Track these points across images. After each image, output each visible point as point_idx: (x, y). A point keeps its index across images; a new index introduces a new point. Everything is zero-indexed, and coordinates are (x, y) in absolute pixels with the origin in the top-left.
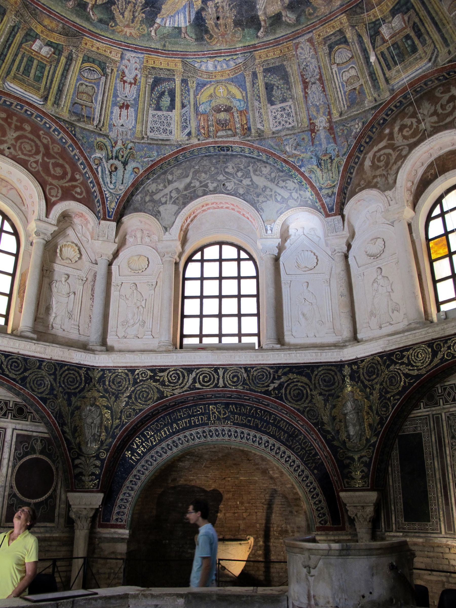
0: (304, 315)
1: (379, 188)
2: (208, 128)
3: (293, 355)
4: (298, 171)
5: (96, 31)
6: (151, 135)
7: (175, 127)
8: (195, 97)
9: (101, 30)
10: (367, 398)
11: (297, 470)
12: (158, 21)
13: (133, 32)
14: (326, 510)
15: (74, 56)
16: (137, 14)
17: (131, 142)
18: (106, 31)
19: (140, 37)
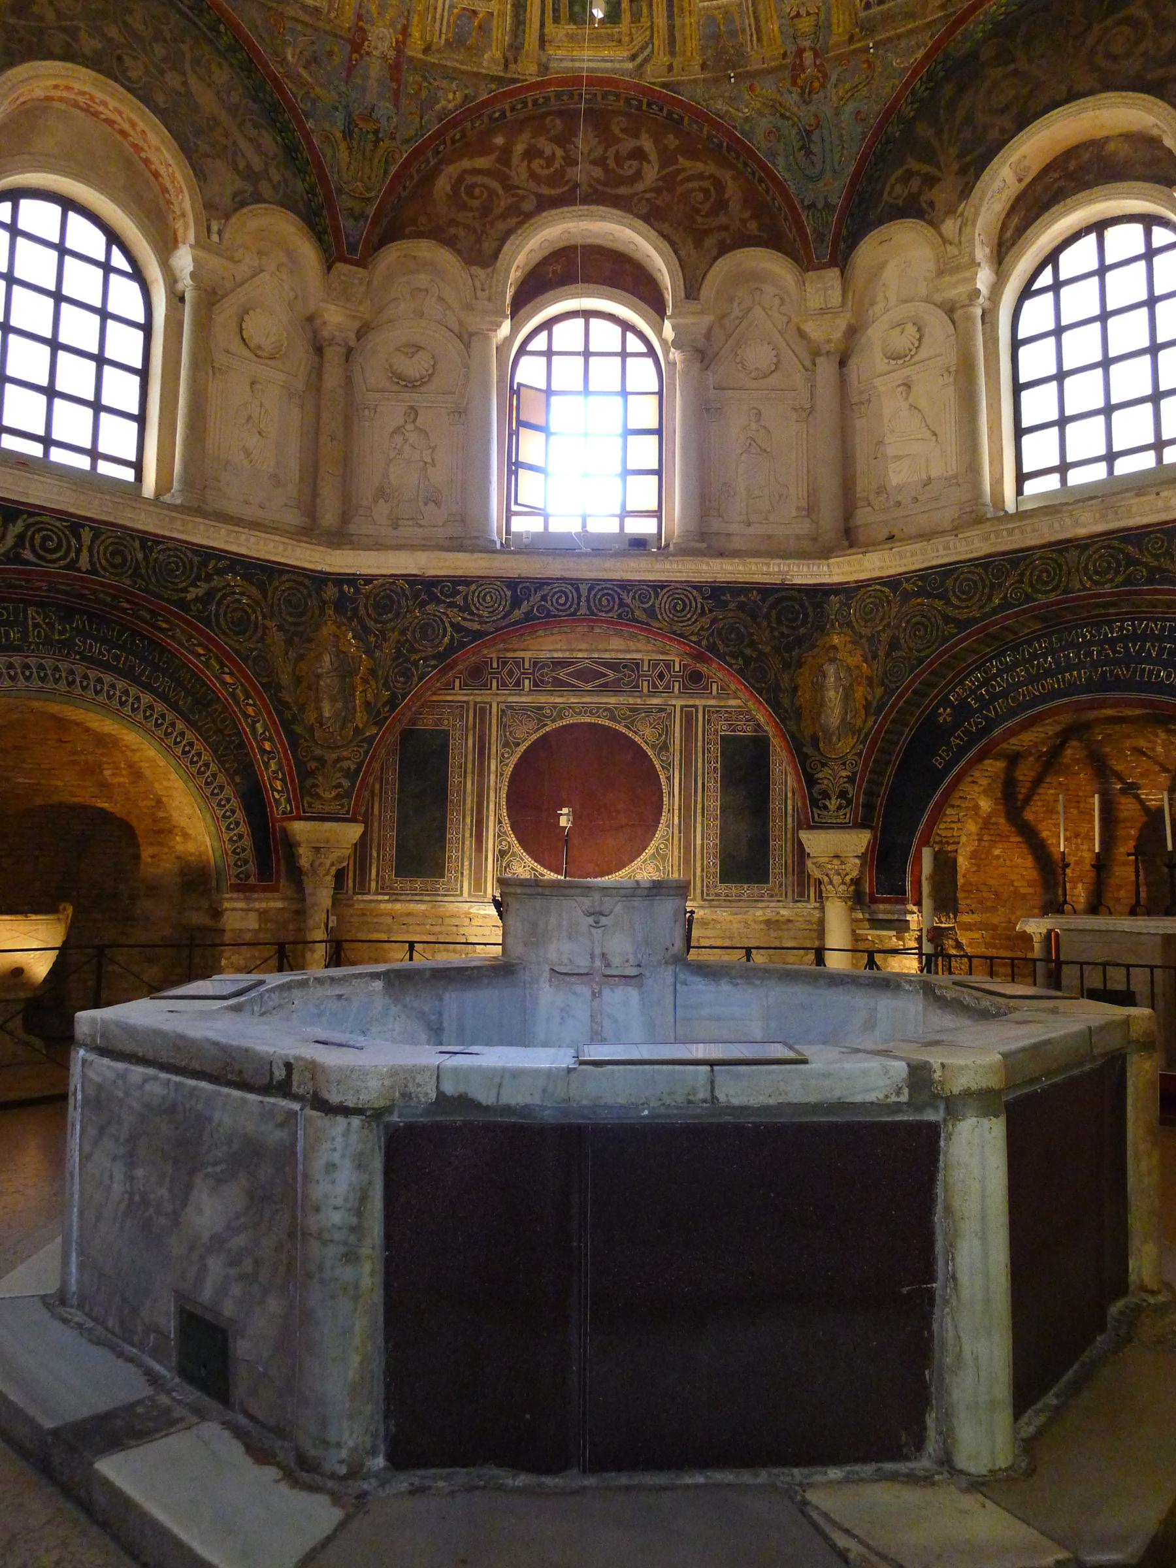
0: (248, 454)
1: (459, 252)
3: (243, 537)
4: (300, 122)
10: (369, 653)
11: (204, 773)
14: (249, 854)
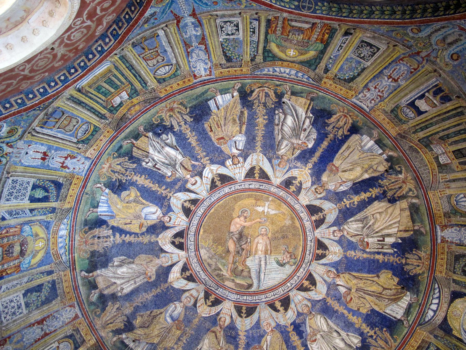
2: (7, 236)
5: (115, 142)
6: (10, 181)
7: (14, 204)
8: (38, 221)
9: (114, 146)
12: (107, 191)
13: (104, 170)
15: (103, 121)
16: (116, 174)
17: (7, 162)
18: (112, 150)
19: (99, 175)
